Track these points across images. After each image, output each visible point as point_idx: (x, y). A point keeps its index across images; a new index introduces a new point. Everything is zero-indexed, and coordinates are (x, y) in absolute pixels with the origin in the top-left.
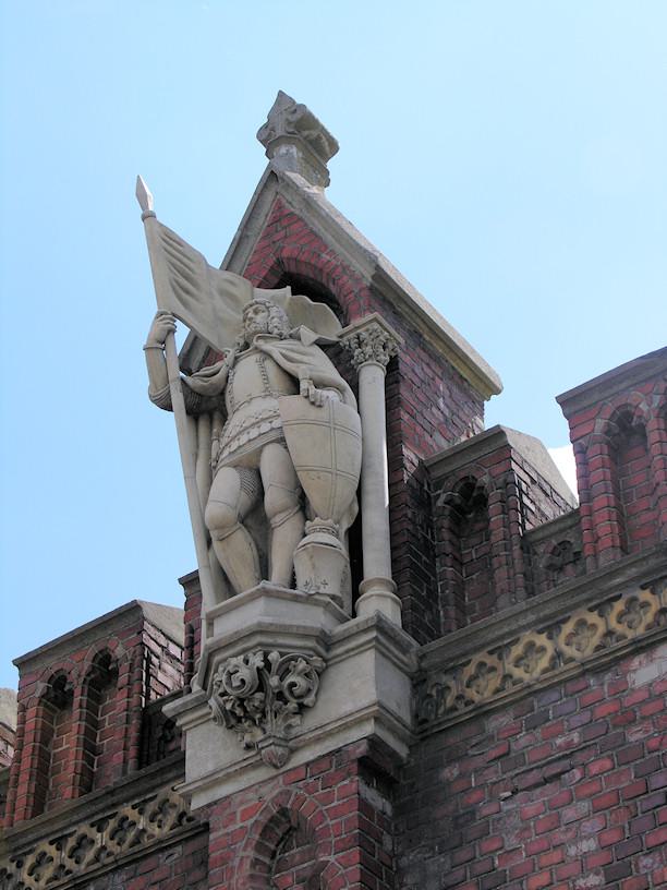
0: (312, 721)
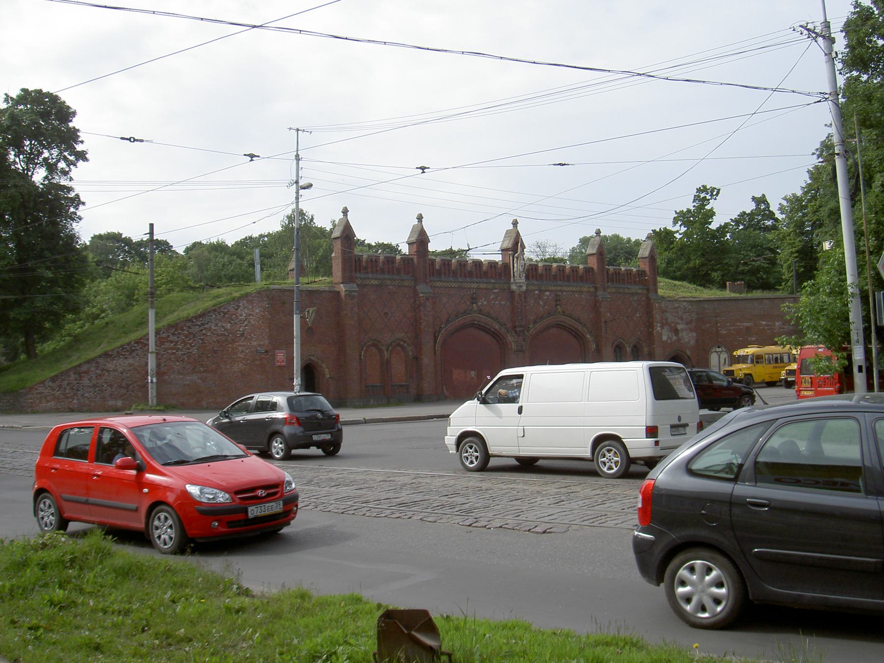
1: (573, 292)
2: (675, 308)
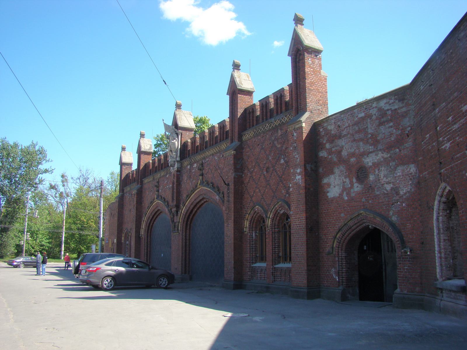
2: (356, 124)
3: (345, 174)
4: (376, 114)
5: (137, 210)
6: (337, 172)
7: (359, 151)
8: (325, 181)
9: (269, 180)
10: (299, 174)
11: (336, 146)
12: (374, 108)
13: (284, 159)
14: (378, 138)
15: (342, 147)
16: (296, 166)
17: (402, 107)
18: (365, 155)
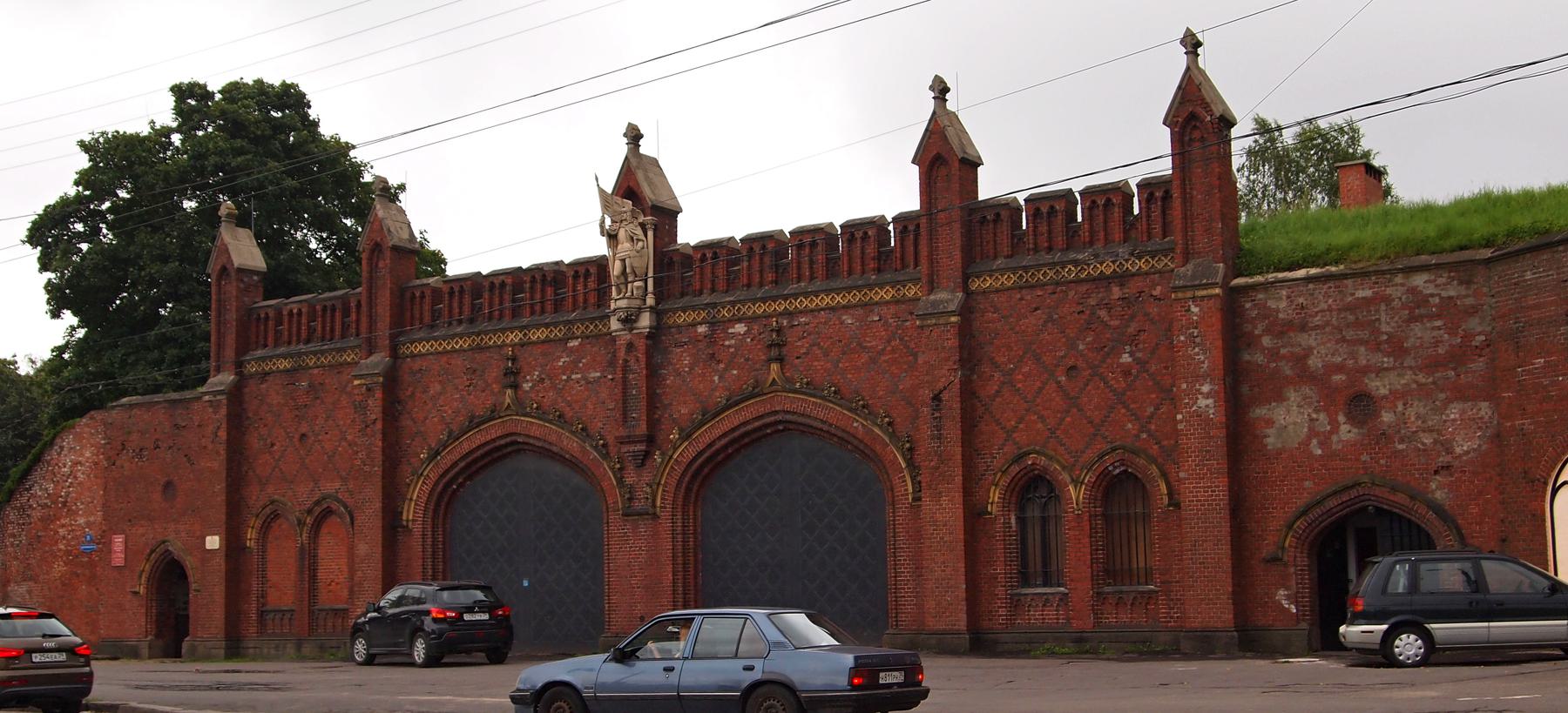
0: (635, 325)
1: (832, 309)
2: (1350, 308)
3: (1316, 404)
4: (1403, 300)
5: (384, 440)
6: (1292, 399)
7: (1356, 362)
8: (1260, 412)
9: (1078, 398)
10: (1207, 396)
11: (1292, 346)
12: (1396, 285)
13: (1131, 354)
14: (1405, 345)
15: (1311, 349)
16: (1200, 378)
17: (1467, 296)
18: (1371, 372)
